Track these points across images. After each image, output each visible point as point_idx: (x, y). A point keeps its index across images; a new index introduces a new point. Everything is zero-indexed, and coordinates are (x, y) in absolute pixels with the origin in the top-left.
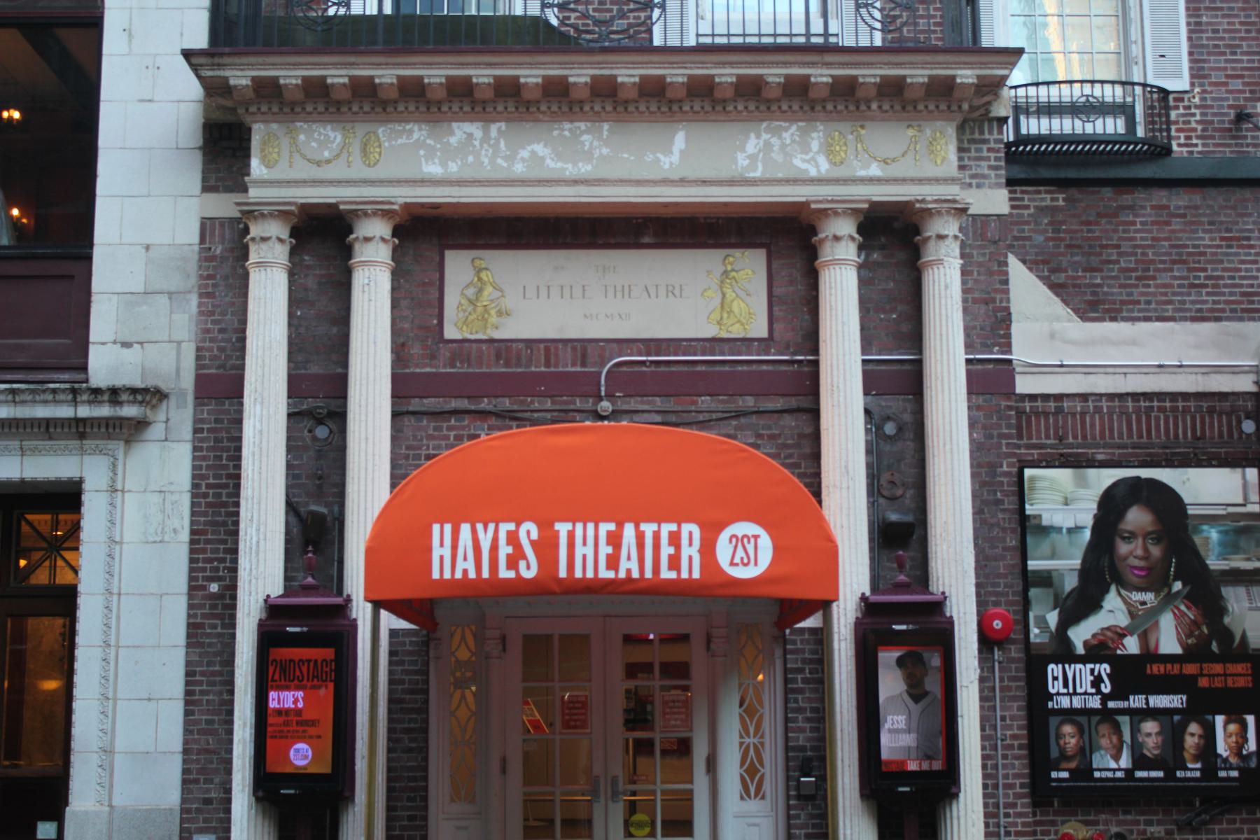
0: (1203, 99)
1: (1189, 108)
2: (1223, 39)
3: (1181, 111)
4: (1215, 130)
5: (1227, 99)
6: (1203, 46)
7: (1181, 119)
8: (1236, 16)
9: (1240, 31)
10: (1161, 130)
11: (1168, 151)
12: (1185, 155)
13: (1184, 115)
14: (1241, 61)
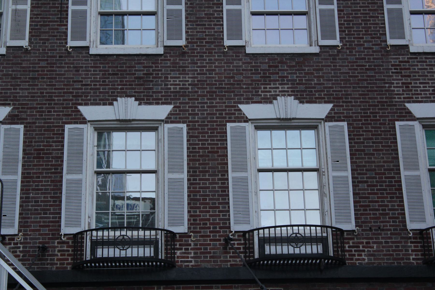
1: (17, 244)
2: (40, 206)
3: (12, 246)
4: (30, 256)
5: (39, 239)
6: (28, 210)
8: (50, 193)
9: (50, 201)
14: (49, 218)
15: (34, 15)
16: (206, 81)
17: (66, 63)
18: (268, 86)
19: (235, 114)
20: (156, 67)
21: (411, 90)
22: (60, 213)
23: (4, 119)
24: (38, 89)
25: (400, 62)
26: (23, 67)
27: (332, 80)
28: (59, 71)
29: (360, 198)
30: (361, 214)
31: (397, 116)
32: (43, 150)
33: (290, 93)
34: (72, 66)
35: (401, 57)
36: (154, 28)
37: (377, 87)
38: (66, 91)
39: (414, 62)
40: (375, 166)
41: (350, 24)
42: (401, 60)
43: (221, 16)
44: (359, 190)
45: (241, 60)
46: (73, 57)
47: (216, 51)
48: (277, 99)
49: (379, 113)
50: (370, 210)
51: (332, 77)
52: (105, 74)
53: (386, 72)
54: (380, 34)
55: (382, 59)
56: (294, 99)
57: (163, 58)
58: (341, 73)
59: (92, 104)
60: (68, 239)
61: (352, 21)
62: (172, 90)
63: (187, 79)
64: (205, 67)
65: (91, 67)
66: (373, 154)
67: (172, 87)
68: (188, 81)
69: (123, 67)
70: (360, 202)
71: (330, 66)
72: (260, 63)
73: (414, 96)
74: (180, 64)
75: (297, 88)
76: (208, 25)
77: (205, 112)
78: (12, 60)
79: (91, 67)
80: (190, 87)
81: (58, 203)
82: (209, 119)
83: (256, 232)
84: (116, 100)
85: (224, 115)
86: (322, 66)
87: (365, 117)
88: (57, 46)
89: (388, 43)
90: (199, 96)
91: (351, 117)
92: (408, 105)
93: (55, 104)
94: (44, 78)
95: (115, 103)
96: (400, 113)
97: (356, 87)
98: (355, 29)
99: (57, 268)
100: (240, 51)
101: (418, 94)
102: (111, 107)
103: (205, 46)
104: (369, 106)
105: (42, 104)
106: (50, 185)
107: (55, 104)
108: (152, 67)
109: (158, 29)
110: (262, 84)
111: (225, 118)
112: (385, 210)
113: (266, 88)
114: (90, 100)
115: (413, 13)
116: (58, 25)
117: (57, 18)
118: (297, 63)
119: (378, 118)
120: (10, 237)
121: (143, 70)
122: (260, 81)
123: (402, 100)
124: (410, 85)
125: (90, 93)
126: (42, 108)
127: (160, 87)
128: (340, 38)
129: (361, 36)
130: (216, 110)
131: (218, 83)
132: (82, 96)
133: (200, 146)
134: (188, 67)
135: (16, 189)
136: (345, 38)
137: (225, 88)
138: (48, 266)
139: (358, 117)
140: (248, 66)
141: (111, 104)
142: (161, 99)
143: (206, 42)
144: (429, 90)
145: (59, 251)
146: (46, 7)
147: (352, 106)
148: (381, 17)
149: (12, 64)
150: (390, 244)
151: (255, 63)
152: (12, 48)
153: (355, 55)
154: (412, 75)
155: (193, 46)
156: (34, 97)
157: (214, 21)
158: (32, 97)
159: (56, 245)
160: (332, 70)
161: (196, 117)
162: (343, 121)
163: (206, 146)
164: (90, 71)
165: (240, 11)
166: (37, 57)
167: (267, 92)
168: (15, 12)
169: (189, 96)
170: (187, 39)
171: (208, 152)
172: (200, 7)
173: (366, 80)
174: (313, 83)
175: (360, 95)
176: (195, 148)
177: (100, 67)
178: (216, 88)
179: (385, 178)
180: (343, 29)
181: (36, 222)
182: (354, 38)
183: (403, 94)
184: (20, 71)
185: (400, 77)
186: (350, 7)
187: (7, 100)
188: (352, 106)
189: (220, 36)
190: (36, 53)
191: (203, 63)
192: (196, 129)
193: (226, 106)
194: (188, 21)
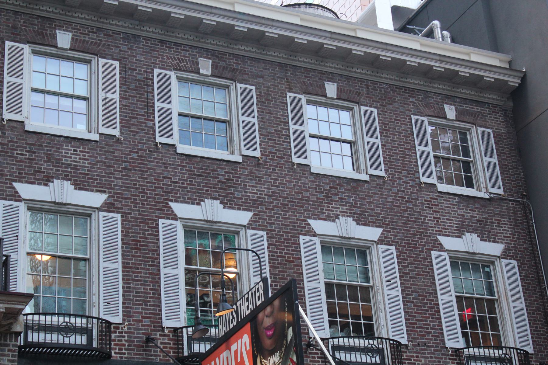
0: (129, 328)
1: (122, 333)
2: (141, 297)
3: (118, 334)
4: (135, 346)
5: (142, 329)
6: (130, 300)
7: (117, 339)
8: (148, 285)
9: (150, 293)
10: (106, 344)
11: (110, 356)
12: (119, 359)
13: (119, 337)
14: (150, 309)
17: (155, 158)
18: (331, 206)
21: (441, 225)
22: (160, 306)
23: (101, 206)
25: (431, 198)
26: (116, 157)
27: (380, 207)
29: (409, 316)
30: (411, 331)
32: (140, 241)
33: (349, 214)
35: (431, 194)
37: (415, 218)
39: (441, 200)
40: (418, 289)
44: (408, 308)
45: (306, 178)
46: (161, 153)
50: (417, 327)
51: (380, 204)
52: (191, 174)
54: (415, 171)
57: (241, 166)
58: (387, 202)
59: (182, 202)
60: (169, 332)
62: (251, 198)
63: (263, 189)
64: (278, 180)
65: (179, 165)
66: (416, 278)
67: (251, 195)
68: (264, 191)
69: (206, 169)
70: (409, 320)
71: (378, 194)
72: (323, 183)
76: (278, 141)
78: (105, 148)
79: (179, 165)
80: (266, 197)
81: (157, 296)
83: (184, 330)
84: (204, 201)
90: (274, 206)
91: (397, 242)
92: (439, 238)
94: (136, 170)
95: (202, 203)
99: (160, 359)
101: (445, 229)
103: (276, 160)
105: (135, 196)
106: (148, 277)
107: (147, 197)
108: (232, 173)
110: (325, 203)
111: (297, 230)
112: (427, 328)
114: (179, 197)
116: (145, 119)
117: (145, 112)
118: (353, 187)
120: (114, 325)
121: (225, 175)
122: (324, 200)
123: (434, 232)
125: (179, 190)
128: (385, 170)
130: (290, 222)
133: (278, 254)
134: (263, 178)
135: (117, 277)
137: (295, 202)
138: (153, 357)
141: (199, 204)
142: (242, 206)
143: (277, 157)
144: (453, 227)
145: (161, 343)
146: (133, 100)
149: (105, 151)
150: (434, 359)
155: (266, 159)
156: (127, 187)
158: (126, 187)
159: (158, 337)
160: (380, 197)
162: (391, 245)
163: (284, 255)
164: (178, 169)
166: (127, 147)
168: (105, 99)
170: (261, 151)
171: (286, 261)
172: (269, 123)
173: (407, 211)
175: (403, 223)
176: (274, 256)
177: (186, 166)
178: (288, 201)
179: (427, 300)
181: (138, 313)
185: (431, 212)
187: (102, 187)
188: (398, 233)
192: (273, 238)
193: (297, 220)
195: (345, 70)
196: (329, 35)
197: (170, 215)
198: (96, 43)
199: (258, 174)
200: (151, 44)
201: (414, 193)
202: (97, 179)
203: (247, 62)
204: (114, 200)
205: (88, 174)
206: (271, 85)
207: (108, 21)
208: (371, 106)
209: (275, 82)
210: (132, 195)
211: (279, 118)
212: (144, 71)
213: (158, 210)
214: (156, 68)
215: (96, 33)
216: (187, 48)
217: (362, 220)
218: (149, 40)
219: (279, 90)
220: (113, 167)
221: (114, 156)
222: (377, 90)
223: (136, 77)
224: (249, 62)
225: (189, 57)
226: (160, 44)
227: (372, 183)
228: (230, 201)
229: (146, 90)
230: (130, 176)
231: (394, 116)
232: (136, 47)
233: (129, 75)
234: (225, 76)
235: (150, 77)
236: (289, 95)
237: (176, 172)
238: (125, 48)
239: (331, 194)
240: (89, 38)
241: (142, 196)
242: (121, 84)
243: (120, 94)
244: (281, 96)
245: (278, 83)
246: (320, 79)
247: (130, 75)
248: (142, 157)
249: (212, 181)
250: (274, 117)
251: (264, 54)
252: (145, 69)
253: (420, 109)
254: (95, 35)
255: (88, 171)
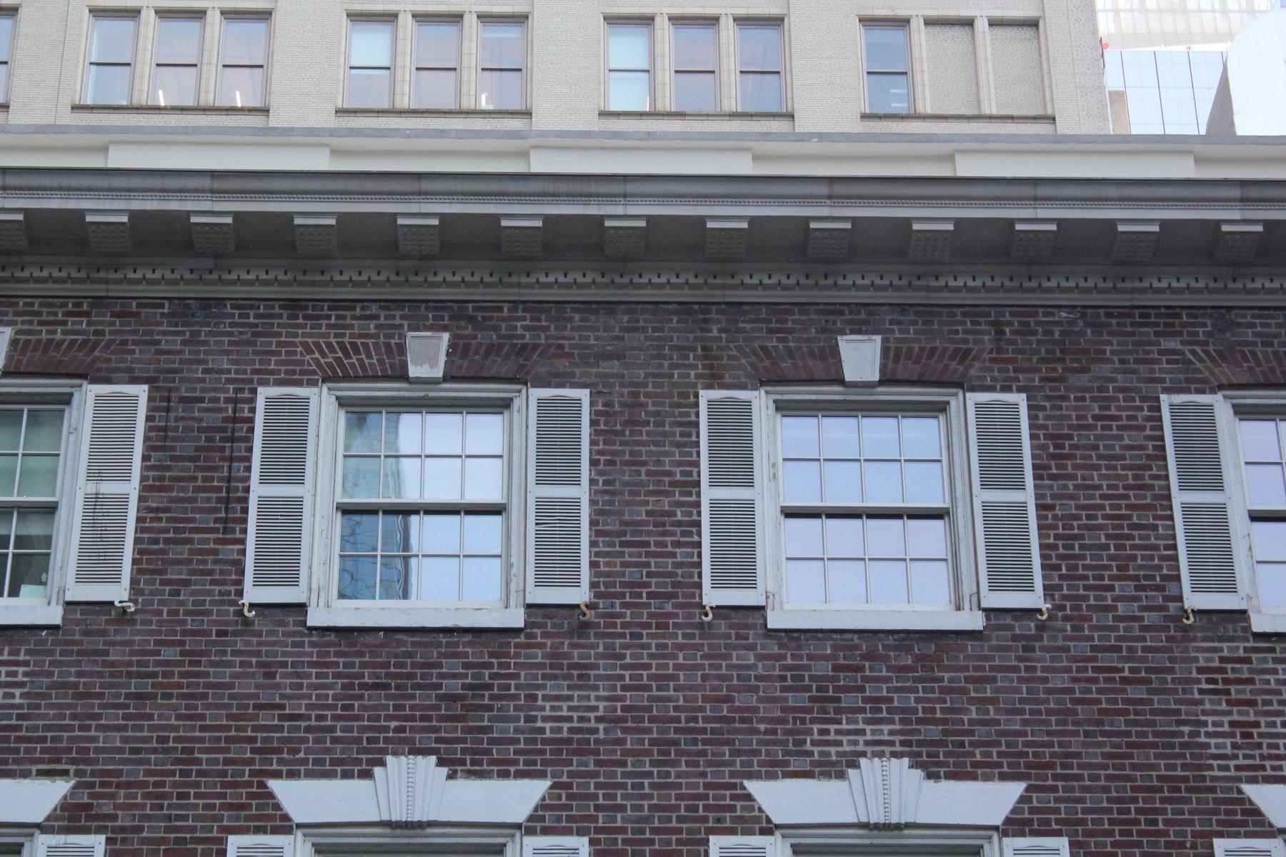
15: (150, 510)
16: (649, 709)
18: (833, 727)
19: (732, 808)
20: (500, 665)
21: (1259, 746)
23: (48, 819)
24: (152, 728)
25: (1222, 660)
26: (112, 664)
27: (1022, 712)
28: (216, 675)
31: (1219, 823)
33: (898, 748)
34: (254, 660)
35: (1225, 645)
36: (498, 552)
37: (1156, 734)
38: (233, 733)
39: (1265, 660)
41: (1072, 547)
42: (1226, 653)
43: (695, 517)
45: (752, 647)
46: (259, 634)
47: (680, 621)
48: (858, 767)
49: (1164, 812)
51: (1022, 700)
52: (351, 687)
53: (1184, 689)
54: (1164, 578)
55: (1170, 650)
56: (911, 767)
58: (1049, 691)
59: (310, 775)
61: (1082, 537)
62: (548, 735)
63: (593, 703)
65: (312, 664)
67: (548, 725)
68: (596, 709)
69: (403, 665)
71: (1015, 669)
72: (810, 657)
73: (1268, 763)
74: (572, 658)
75: (919, 732)
76: (657, 544)
77: (646, 803)
78: (81, 643)
79: (312, 664)
80: (601, 726)
82: (657, 824)
84: (382, 763)
85: (701, 813)
86: (992, 669)
87: (1122, 822)
88: (213, 603)
89: (1188, 604)
90: (626, 753)
91: (1082, 822)
92: (1250, 790)
93: (201, 773)
94: (170, 696)
96: (1227, 812)
97: (1093, 734)
98: (1088, 562)
100: (750, 621)
102: (366, 783)
103: (647, 606)
104: (1134, 789)
105: (161, 773)
107: (201, 773)
108: (490, 666)
109: (509, 556)
110: (813, 721)
111: (705, 819)
113: (827, 732)
114: (304, 762)
115: (1257, 517)
116: (217, 541)
117: (216, 520)
118: (918, 659)
119: (1161, 826)
121: (465, 676)
123: (1233, 773)
124: (1255, 731)
125: (306, 740)
126: (163, 784)
127: (512, 725)
128: (1045, 587)
129: (1106, 582)
130: (680, 797)
131: (683, 715)
132: (280, 751)
134: (596, 667)
136: (1060, 588)
137: (704, 731)
139: (1101, 821)
140: (774, 666)
141: (366, 775)
142: (515, 762)
143: (650, 595)
147: (1085, 789)
148: (1166, 528)
149: (80, 653)
151: (794, 657)
152: (79, 608)
153: (1091, 638)
154: (1259, 698)
155: (612, 605)
157: (673, 534)
158: (132, 751)
160: (1021, 680)
161: (619, 815)
162: (1058, 833)
164: (308, 676)
165: (749, 507)
167: (828, 743)
168: (95, 501)
169: (597, 753)
170: (593, 585)
172: (632, 493)
173: (1124, 712)
174: (965, 718)
175: (1106, 756)
177: (336, 664)
178: (677, 731)
180: (1054, 561)
182: (1086, 588)
183: (1236, 757)
184: (100, 675)
185: (1224, 707)
186: (1072, 497)
187: (58, 761)
188: (1085, 789)
189: (692, 577)
190: (151, 623)
191: (640, 656)
193: (708, 786)
194: (599, 533)
195: (1115, 289)
196: (823, 189)
197: (270, 818)
198: (85, 342)
199: (580, 657)
200: (257, 316)
201: (1157, 650)
202: (44, 740)
203: (571, 319)
204: (91, 796)
205: (18, 728)
206: (647, 375)
207: (119, 275)
208: (1006, 389)
209: (661, 366)
210: (149, 773)
211: (669, 474)
212: (227, 400)
213: (231, 807)
214: (264, 383)
215: (86, 314)
216: (374, 310)
217: (943, 759)
218: (252, 307)
219: (676, 385)
220: (100, 696)
221: (105, 664)
222: (1035, 333)
223: (201, 420)
224: (577, 316)
225: (376, 336)
226: (285, 313)
227: (994, 634)
228: (474, 751)
229: (227, 453)
230: (150, 717)
231: (1095, 405)
232: (210, 334)
233: (177, 419)
234: (493, 373)
235: (246, 414)
236: (705, 396)
237: (300, 686)
238: (176, 343)
239: (836, 689)
240: (65, 333)
241: (184, 773)
242: (149, 449)
243: (143, 479)
244: (678, 405)
245: (673, 366)
246: (824, 330)
247: (183, 419)
248: (193, 656)
249: (419, 697)
250: (649, 473)
251: (623, 286)
252: (231, 394)
253: (1197, 371)
254: (85, 320)
255: (19, 717)
